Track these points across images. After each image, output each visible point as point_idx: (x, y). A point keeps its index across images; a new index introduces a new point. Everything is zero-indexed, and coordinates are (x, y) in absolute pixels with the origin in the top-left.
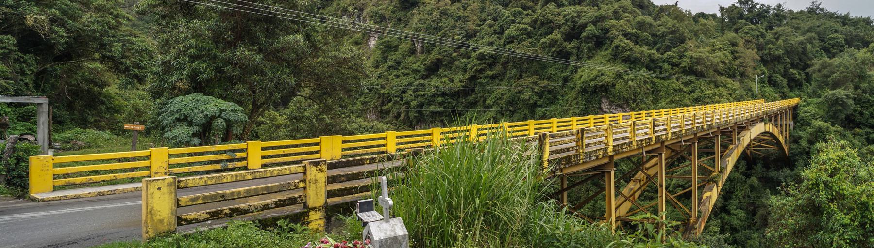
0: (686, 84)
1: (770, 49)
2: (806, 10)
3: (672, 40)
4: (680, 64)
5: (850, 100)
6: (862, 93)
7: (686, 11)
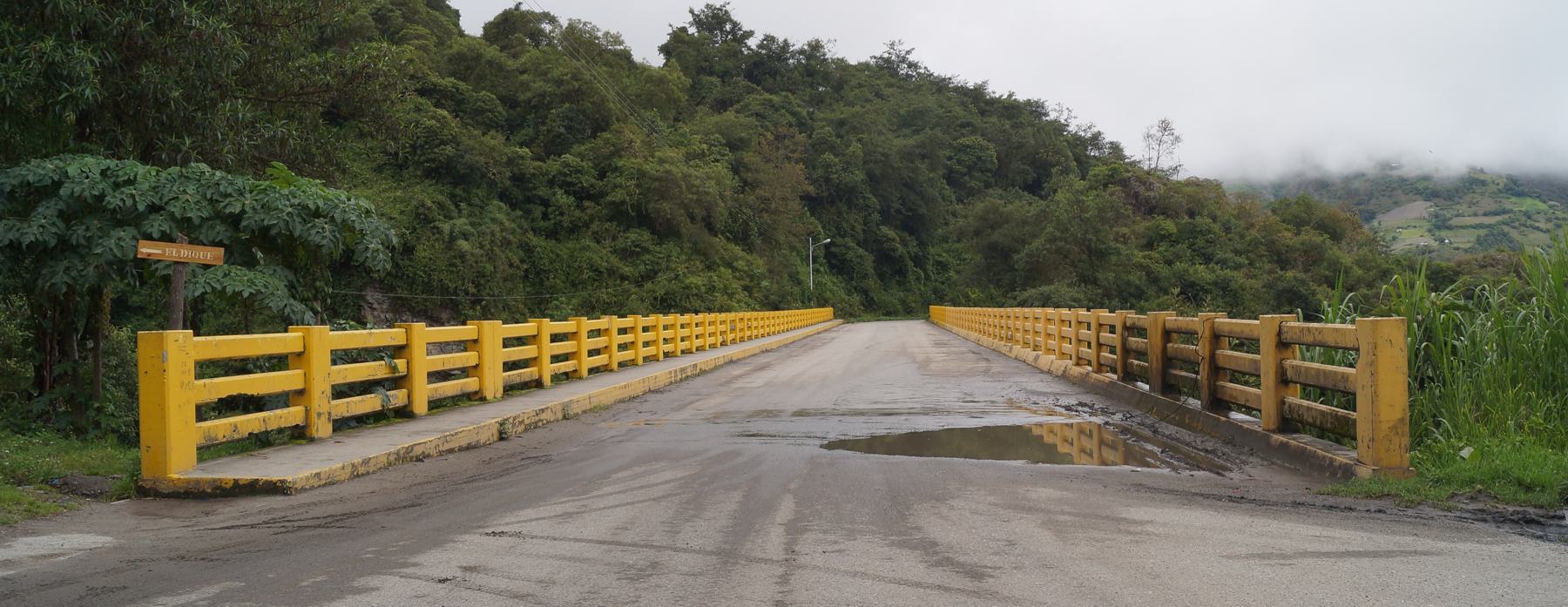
0: (626, 254)
1: (828, 166)
2: (872, 62)
3: (571, 119)
4: (603, 194)
7: (607, 34)
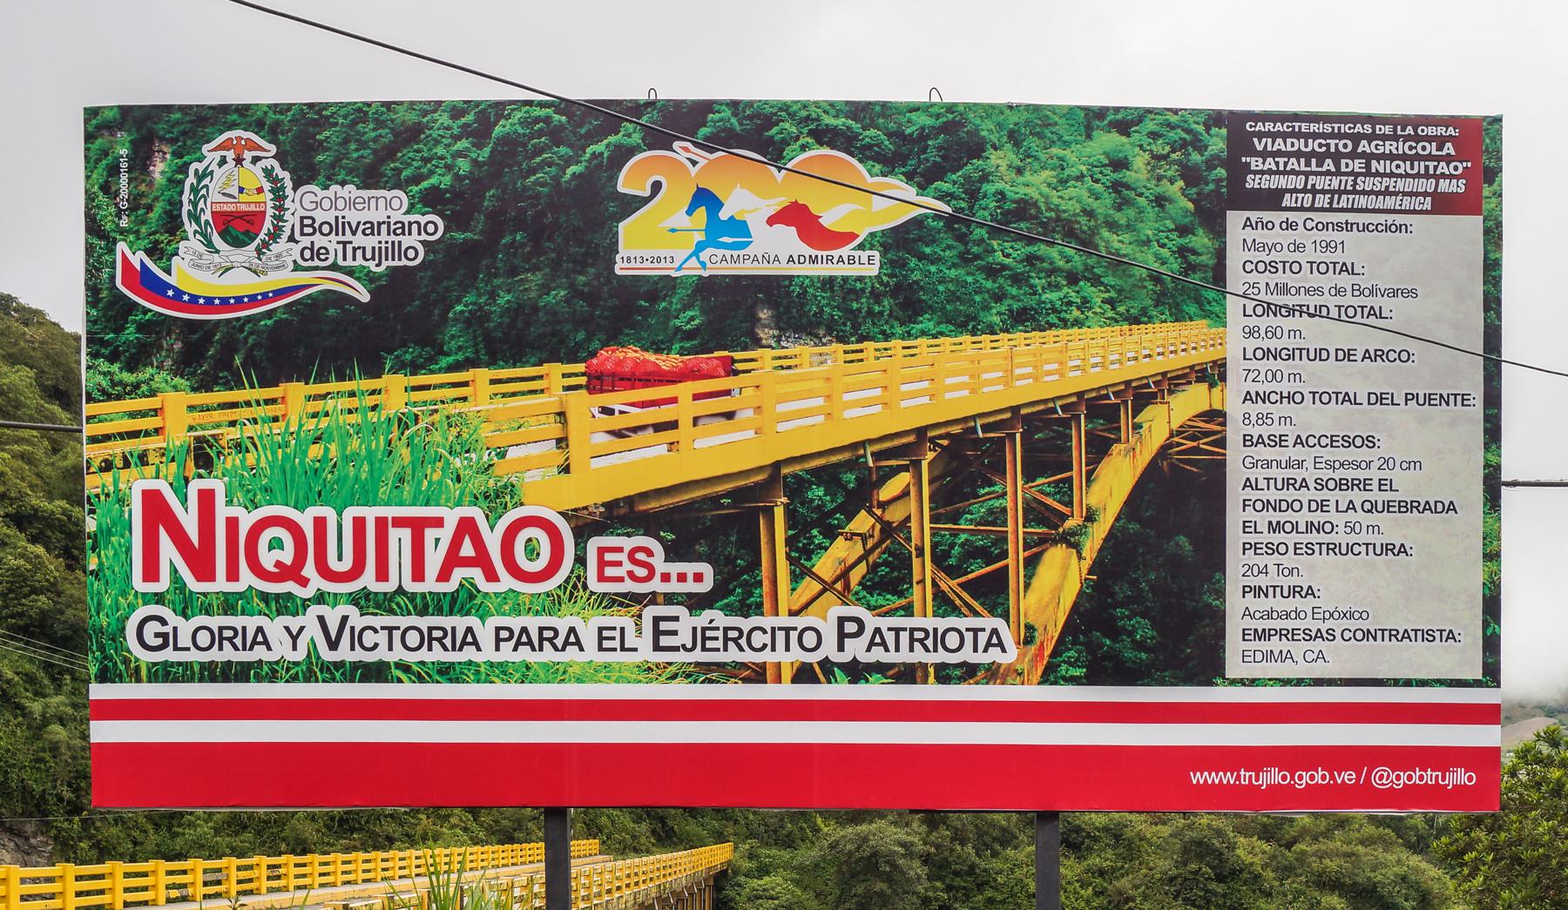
5: (916, 863)
6: (953, 839)
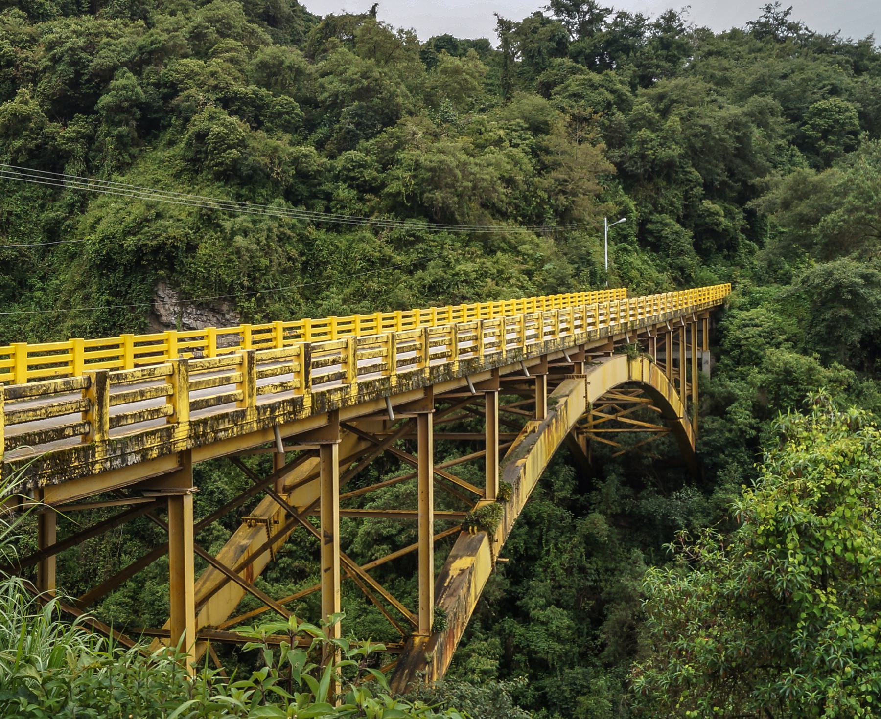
0: (400, 244)
1: (644, 142)
2: (748, 29)
3: (361, 116)
4: (383, 185)
7: (401, 31)
